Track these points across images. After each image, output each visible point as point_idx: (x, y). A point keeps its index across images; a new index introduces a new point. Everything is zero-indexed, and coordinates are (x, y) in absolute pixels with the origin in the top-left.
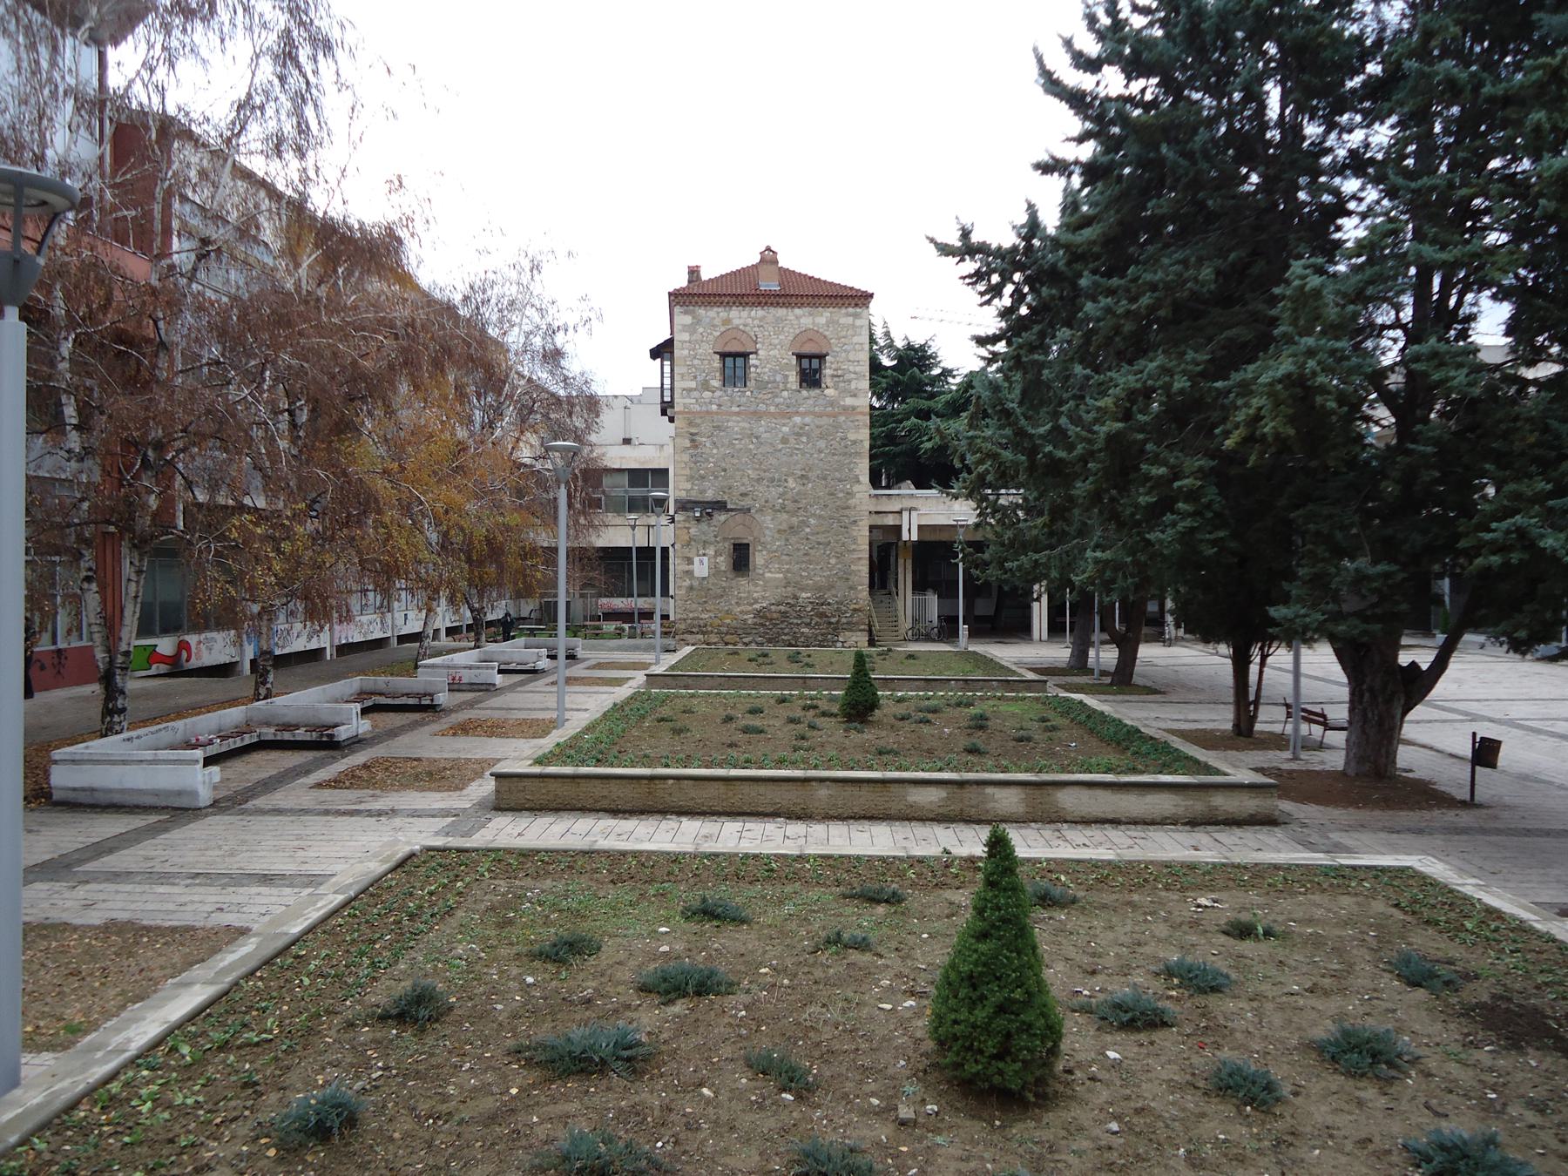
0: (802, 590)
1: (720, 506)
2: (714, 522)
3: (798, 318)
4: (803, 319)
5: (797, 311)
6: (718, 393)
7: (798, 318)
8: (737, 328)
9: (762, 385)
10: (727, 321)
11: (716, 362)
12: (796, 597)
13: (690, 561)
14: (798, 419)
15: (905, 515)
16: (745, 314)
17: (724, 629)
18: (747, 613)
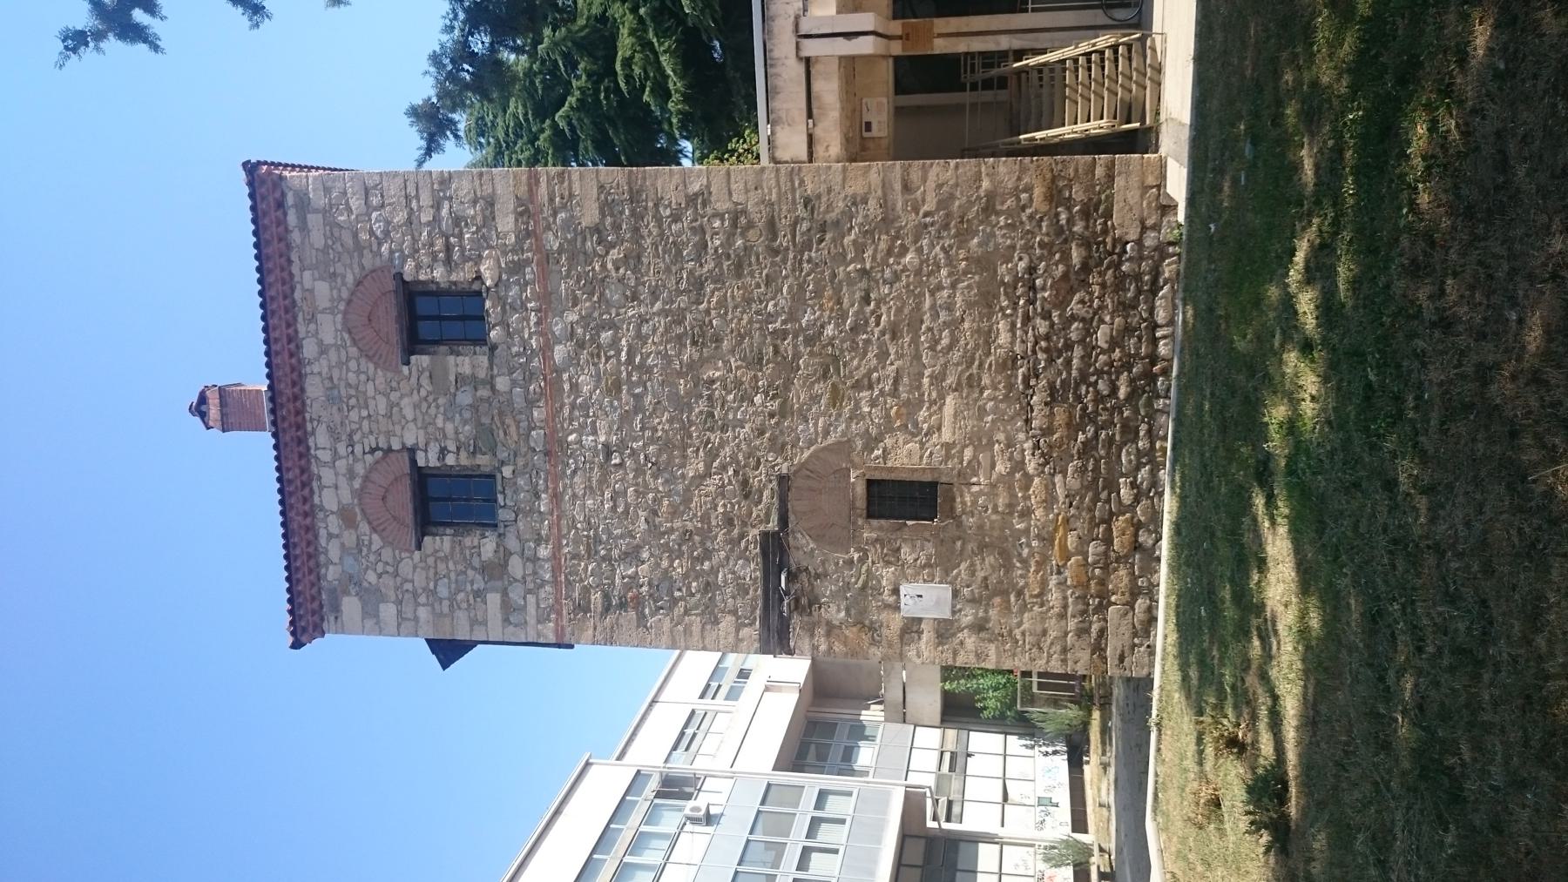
0: (988, 337)
1: (774, 550)
2: (814, 565)
3: (323, 350)
4: (323, 335)
5: (309, 349)
6: (512, 543)
7: (323, 350)
8: (359, 494)
9: (485, 439)
11: (440, 543)
12: (1011, 361)
13: (912, 627)
14: (560, 353)
15: (811, 48)
16: (327, 476)
17: (1093, 549)
18: (1050, 488)
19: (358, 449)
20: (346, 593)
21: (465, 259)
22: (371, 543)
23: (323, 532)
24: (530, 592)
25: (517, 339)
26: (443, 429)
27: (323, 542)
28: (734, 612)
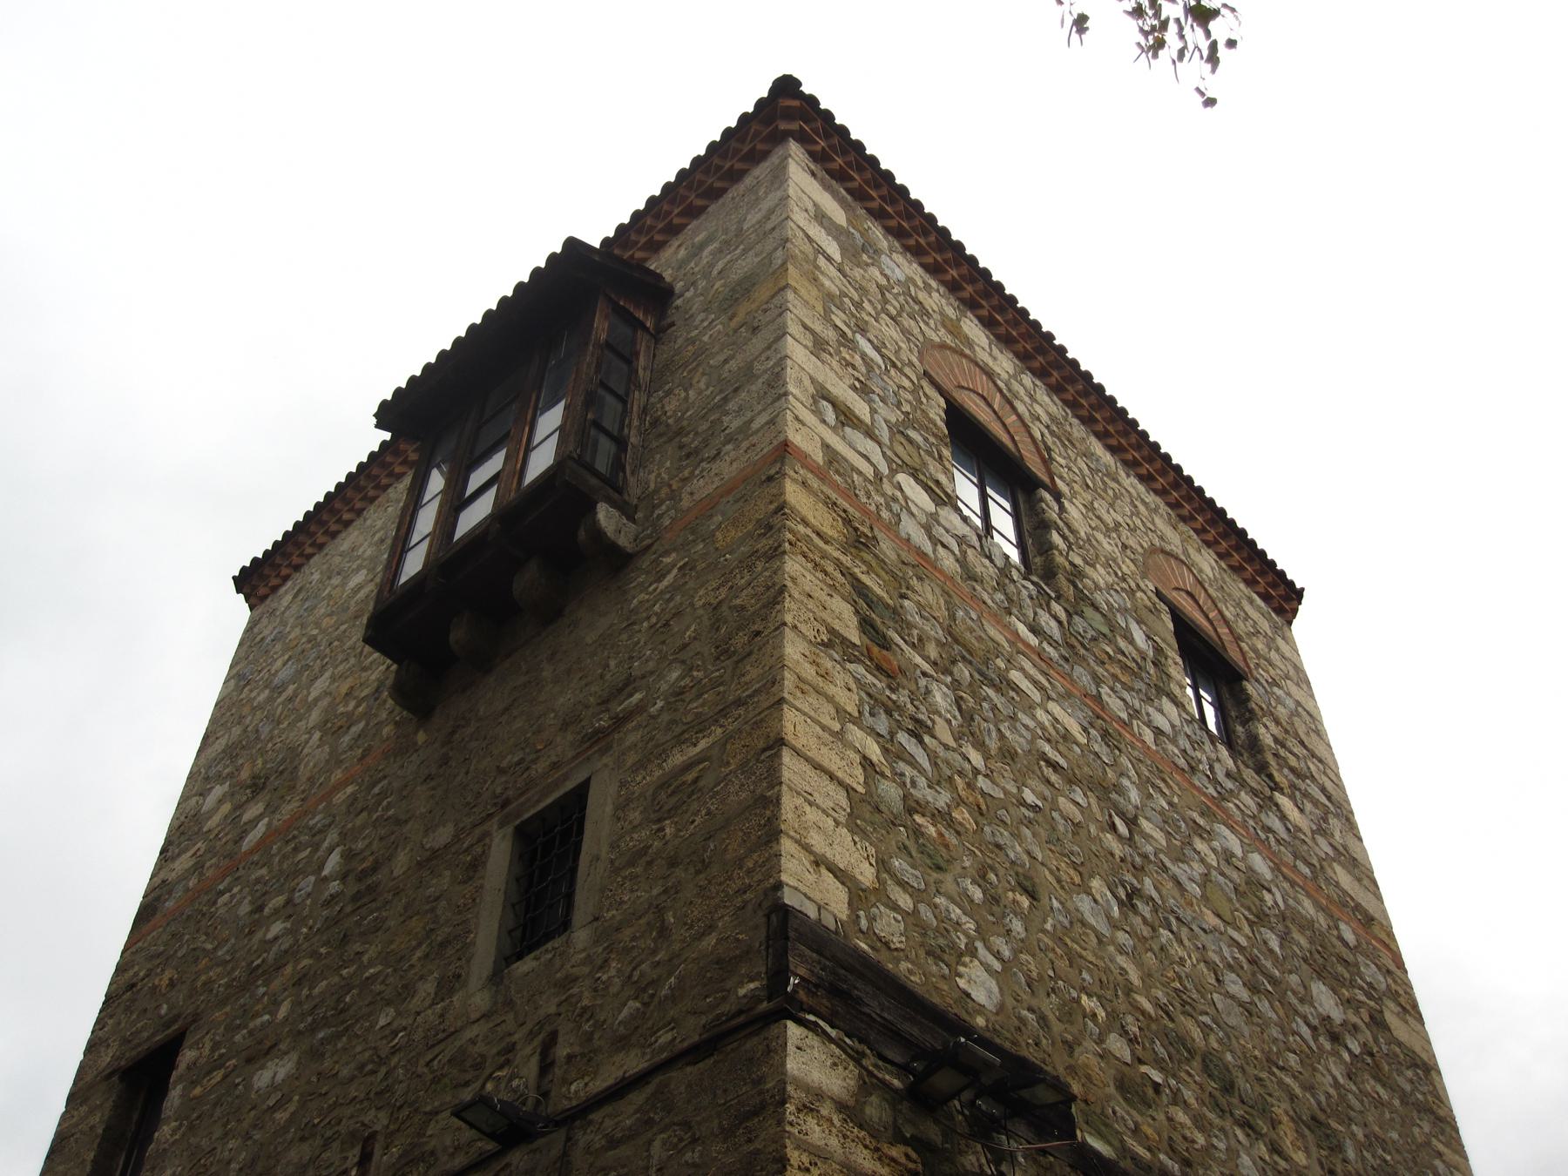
10: (954, 329)
11: (936, 410)
19: (1046, 431)
20: (848, 220)
21: (1293, 786)
22: (927, 324)
23: (934, 284)
24: (878, 476)
25: (1229, 785)
26: (1093, 566)
27: (920, 270)
28: (880, 892)
